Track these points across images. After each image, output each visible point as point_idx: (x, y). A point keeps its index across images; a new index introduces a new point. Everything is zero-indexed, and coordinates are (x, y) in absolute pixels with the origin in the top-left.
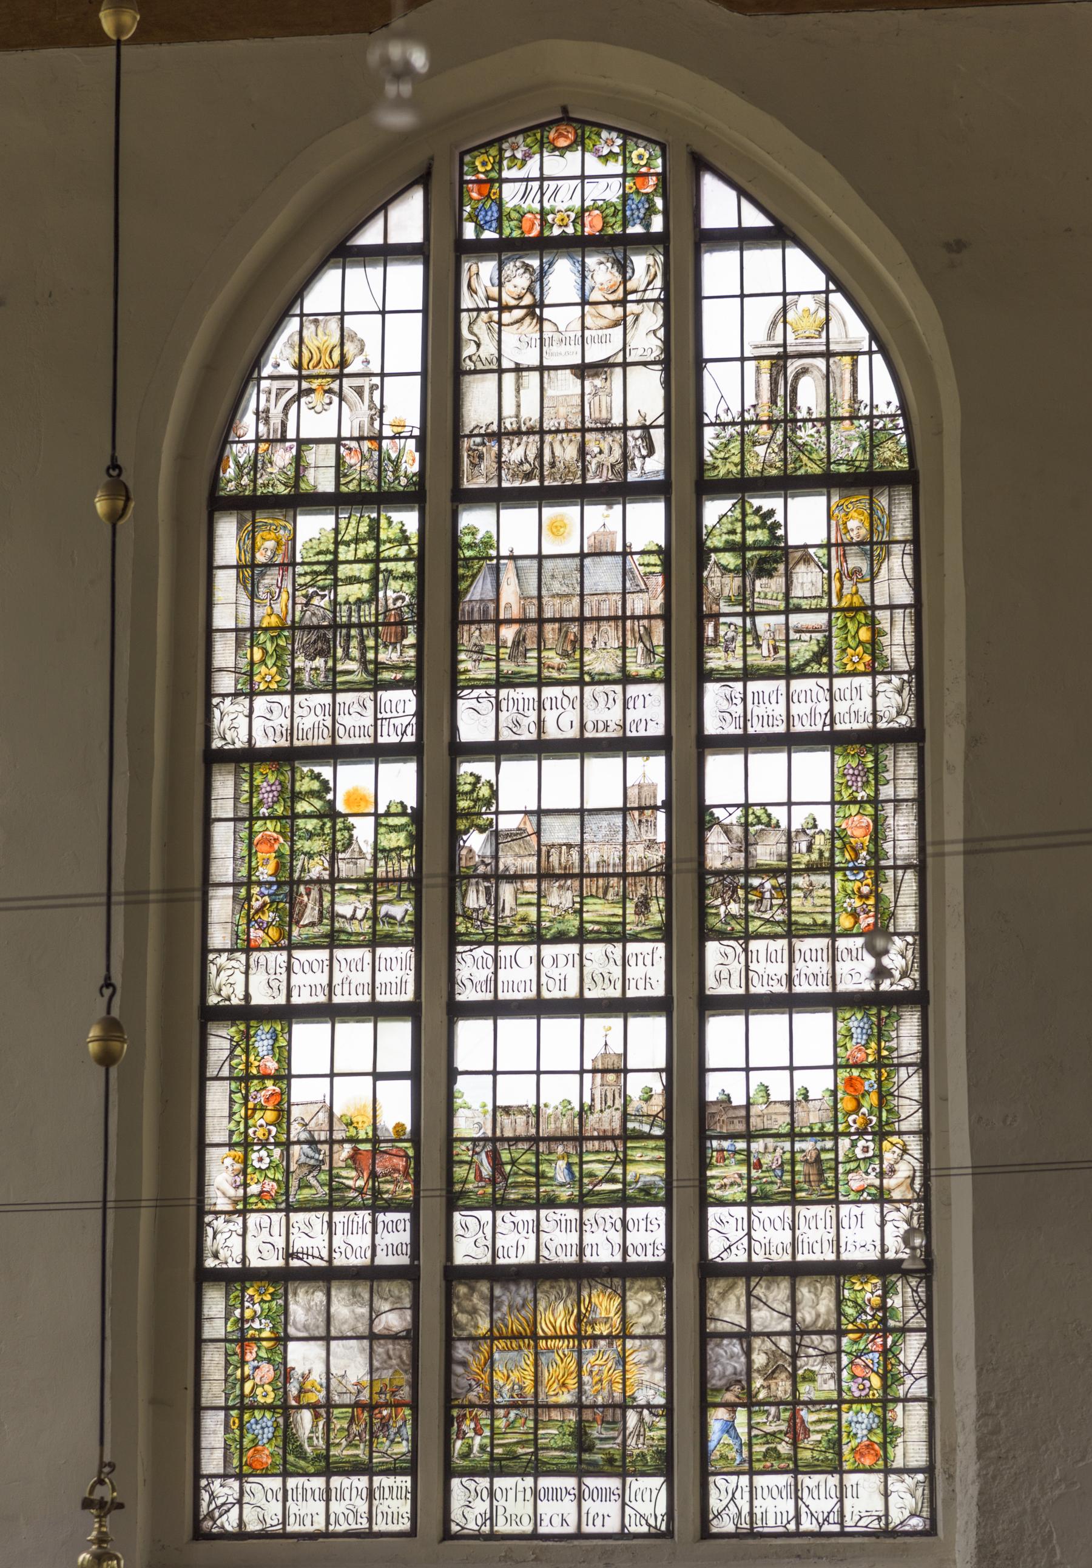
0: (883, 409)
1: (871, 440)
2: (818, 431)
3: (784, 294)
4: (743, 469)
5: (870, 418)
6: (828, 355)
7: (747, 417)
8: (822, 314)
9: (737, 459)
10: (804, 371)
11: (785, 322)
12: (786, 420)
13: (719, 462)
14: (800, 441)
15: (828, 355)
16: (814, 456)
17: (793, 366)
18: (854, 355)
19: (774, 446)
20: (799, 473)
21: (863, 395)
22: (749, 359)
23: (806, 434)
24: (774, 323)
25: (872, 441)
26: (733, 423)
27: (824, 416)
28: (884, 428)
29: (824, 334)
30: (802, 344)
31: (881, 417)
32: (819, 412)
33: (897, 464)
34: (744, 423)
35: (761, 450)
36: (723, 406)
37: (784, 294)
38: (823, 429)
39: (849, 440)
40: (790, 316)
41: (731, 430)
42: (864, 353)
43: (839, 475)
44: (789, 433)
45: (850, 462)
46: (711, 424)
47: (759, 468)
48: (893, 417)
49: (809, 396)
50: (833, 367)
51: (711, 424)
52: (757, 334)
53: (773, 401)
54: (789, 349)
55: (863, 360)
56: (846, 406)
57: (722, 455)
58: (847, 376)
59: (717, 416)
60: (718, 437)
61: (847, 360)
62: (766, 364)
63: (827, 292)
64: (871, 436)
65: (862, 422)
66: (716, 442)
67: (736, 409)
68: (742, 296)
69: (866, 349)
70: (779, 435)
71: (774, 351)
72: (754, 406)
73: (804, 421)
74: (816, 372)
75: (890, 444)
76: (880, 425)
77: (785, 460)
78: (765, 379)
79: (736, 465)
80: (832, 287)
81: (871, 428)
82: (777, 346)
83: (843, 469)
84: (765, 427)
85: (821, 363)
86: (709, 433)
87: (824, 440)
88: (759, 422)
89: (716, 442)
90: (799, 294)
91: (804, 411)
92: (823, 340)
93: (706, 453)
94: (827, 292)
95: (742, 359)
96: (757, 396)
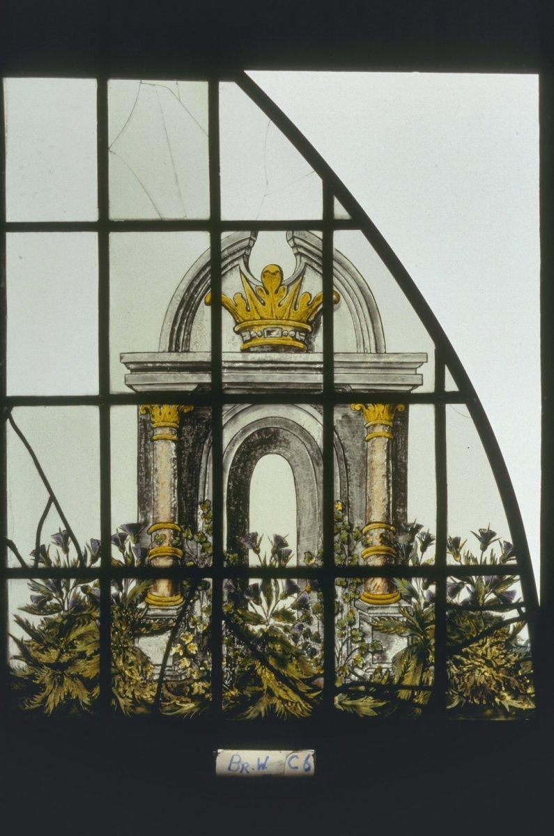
0: (472, 547)
1: (440, 635)
2: (302, 605)
3: (214, 225)
4: (107, 694)
5: (435, 574)
6: (328, 397)
7: (117, 555)
8: (313, 285)
9: (89, 669)
10: (264, 441)
11: (217, 304)
12: (218, 572)
13: (45, 676)
14: (256, 629)
15: (328, 397)
16: (292, 670)
17: (237, 426)
18: (398, 402)
19: (189, 639)
20: (252, 713)
21: (420, 510)
22: (123, 399)
23: (271, 610)
24: (187, 308)
25: (444, 633)
26: (80, 572)
27: (316, 562)
28: (474, 603)
29: (318, 341)
30: (261, 366)
31: (464, 572)
32: (304, 551)
33: (508, 700)
34: (111, 573)
35: (153, 647)
36: (54, 525)
37: (214, 225)
38: (314, 599)
39: (385, 628)
40: (232, 286)
41: (75, 591)
42: (423, 399)
43: (352, 716)
44: (227, 607)
45: (384, 690)
46: (24, 572)
47: (148, 695)
48: (498, 573)
49: (278, 506)
50: (342, 431)
51: (24, 572)
52: (142, 331)
53: (185, 515)
54: (228, 377)
55: (421, 418)
56: (375, 537)
57: (53, 654)
58: (379, 457)
59: (40, 552)
60: (39, 607)
61: (378, 413)
62: (165, 414)
63: (329, 224)
64: (440, 621)
65: (417, 584)
66: (36, 621)
67: (88, 532)
68: (104, 226)
69: (428, 387)
70: (201, 608)
71: (189, 381)
72: (136, 530)
73: (266, 573)
74: (296, 444)
75: (489, 648)
76: (464, 595)
77: (214, 677)
78: (165, 453)
79: (88, 684)
80: (340, 211)
81: (439, 600)
82: (195, 367)
83: (366, 705)
84: (163, 587)
85: (309, 419)
86: (20, 593)
87: (316, 627)
88: (148, 574)
89: (36, 621)
90: (255, 227)
91: (266, 548)
92: (317, 357)
93: (14, 649)
94: (329, 224)
95: (105, 400)
96: (145, 500)
